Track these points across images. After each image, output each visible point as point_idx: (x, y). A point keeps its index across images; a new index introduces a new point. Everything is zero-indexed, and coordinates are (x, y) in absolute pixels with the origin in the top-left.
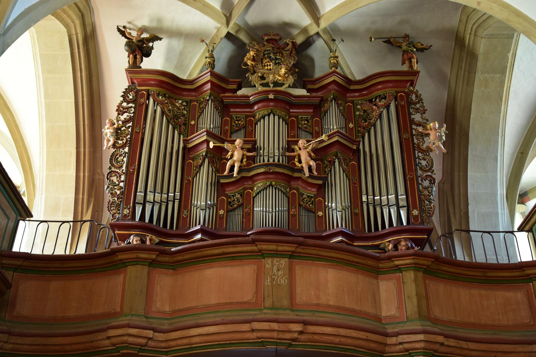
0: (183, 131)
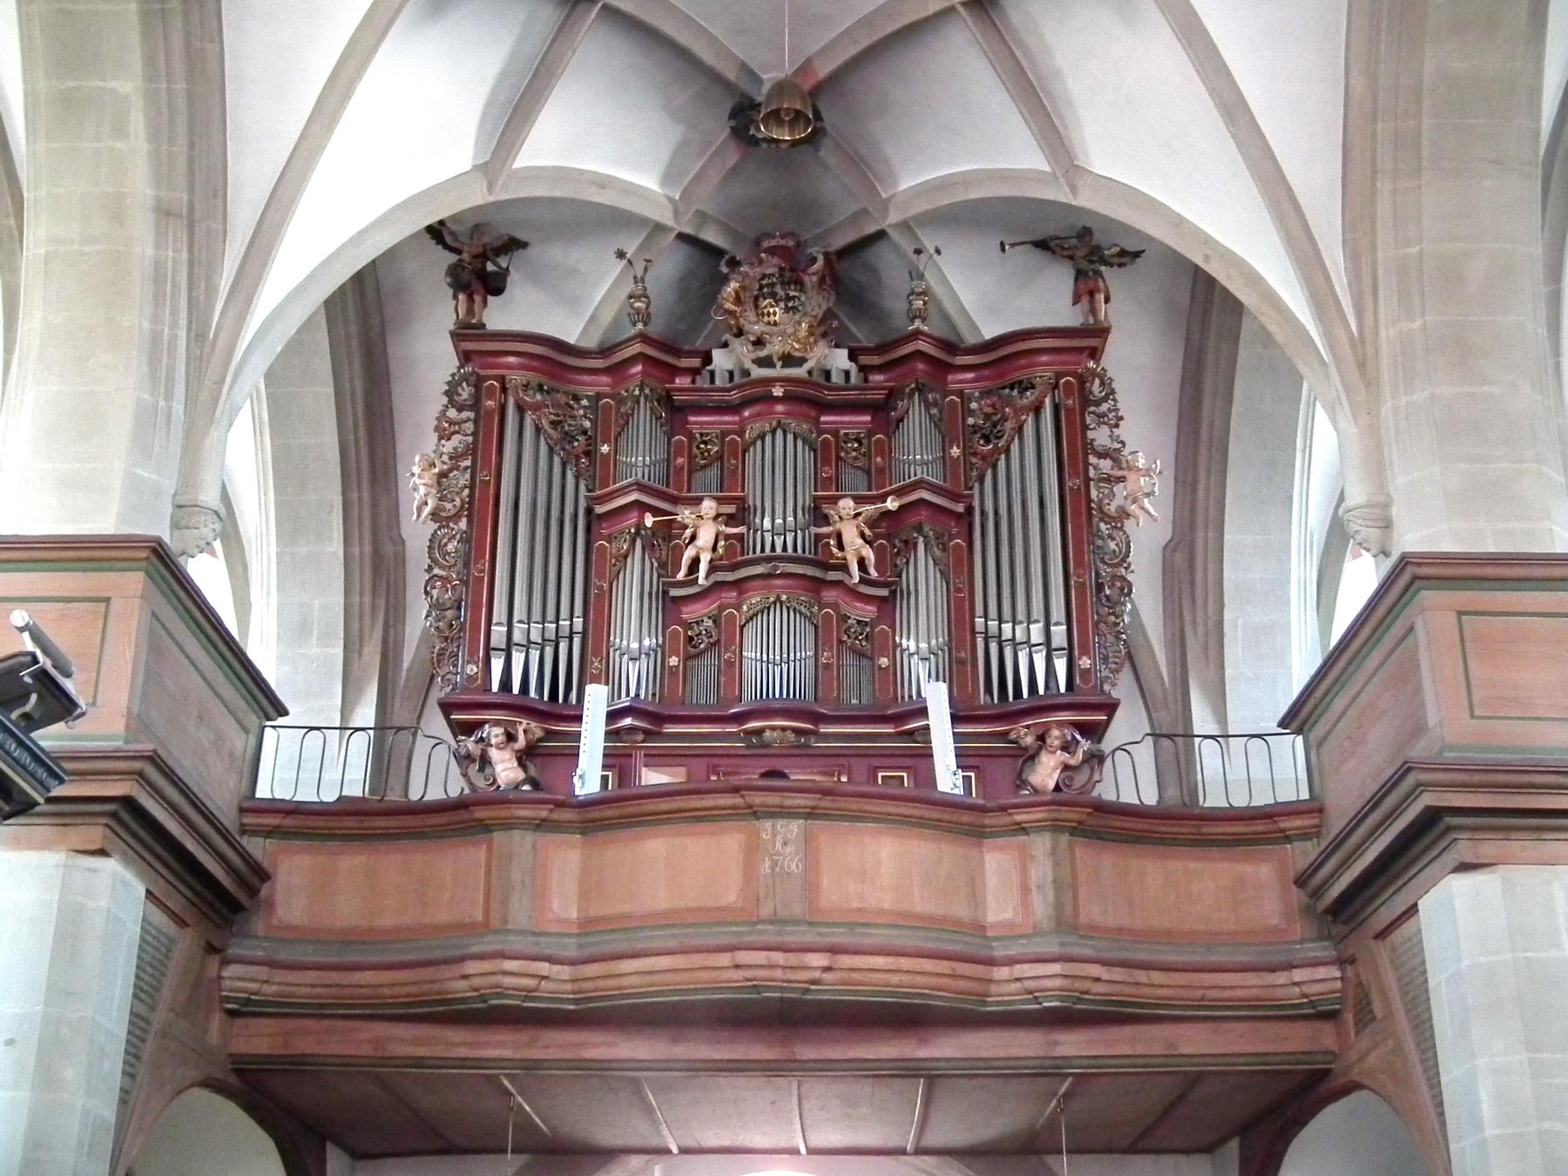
0: (583, 470)
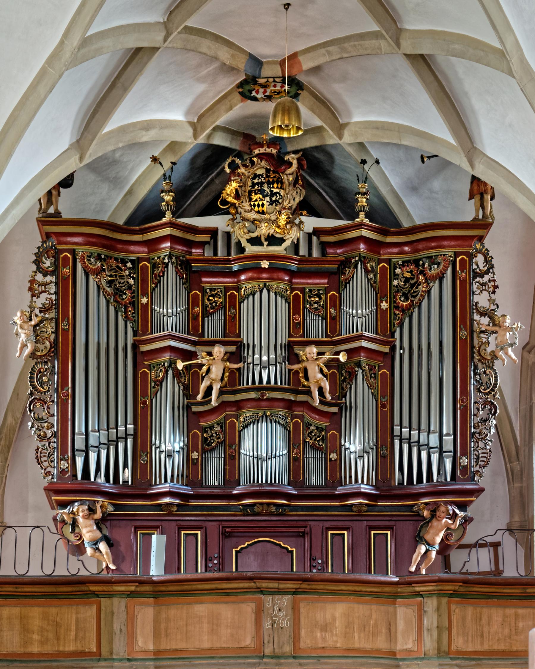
0: (131, 317)
